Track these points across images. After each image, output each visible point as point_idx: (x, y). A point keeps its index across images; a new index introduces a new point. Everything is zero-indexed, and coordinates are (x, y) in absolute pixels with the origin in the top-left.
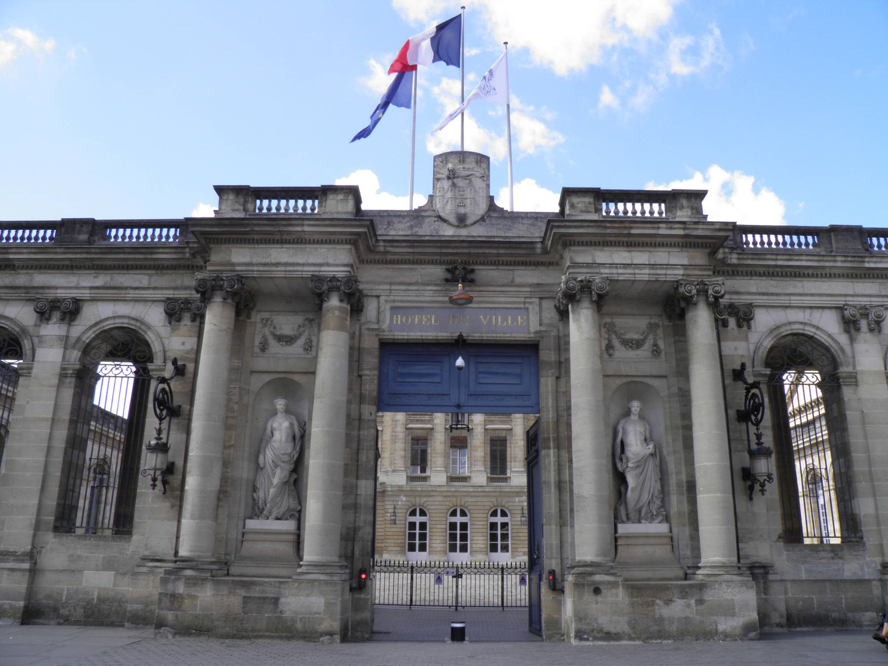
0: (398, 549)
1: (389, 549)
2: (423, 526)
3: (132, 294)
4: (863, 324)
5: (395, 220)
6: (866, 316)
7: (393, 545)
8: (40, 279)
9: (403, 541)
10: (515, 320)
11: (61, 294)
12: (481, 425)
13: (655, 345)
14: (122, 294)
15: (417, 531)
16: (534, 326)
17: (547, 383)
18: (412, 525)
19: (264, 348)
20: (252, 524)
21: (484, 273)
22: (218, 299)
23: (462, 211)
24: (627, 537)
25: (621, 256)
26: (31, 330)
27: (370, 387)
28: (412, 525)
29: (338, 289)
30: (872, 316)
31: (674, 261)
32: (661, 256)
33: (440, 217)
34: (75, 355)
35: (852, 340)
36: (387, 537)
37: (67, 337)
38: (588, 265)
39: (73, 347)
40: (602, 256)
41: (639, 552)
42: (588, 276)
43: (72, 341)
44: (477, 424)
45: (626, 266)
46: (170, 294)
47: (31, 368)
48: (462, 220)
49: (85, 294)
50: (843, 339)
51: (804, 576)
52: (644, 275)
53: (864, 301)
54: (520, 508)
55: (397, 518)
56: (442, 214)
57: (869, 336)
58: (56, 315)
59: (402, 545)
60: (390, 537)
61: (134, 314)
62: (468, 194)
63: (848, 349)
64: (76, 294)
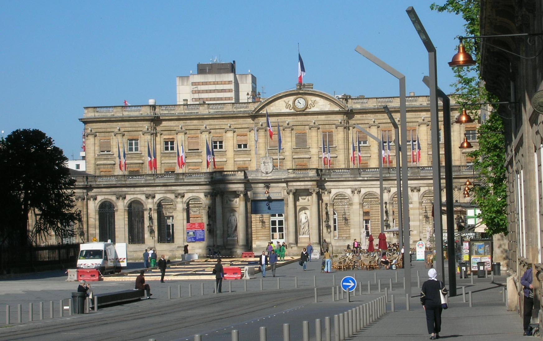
0: (266, 238)
1: (260, 238)
2: (281, 223)
3: (196, 191)
4: (356, 192)
5: (253, 173)
6: (356, 190)
7: (262, 236)
8: (174, 188)
9: (268, 233)
10: (279, 194)
11: (179, 192)
12: (316, 155)
13: (308, 199)
14: (194, 191)
15: (277, 226)
16: (283, 196)
17: (285, 208)
18: (274, 223)
19: (227, 202)
20: (228, 238)
21: (272, 185)
22: (219, 196)
23: (267, 171)
24: (301, 238)
25: (298, 183)
26: (174, 200)
27: (249, 210)
28: (274, 223)
29: (242, 193)
30: (357, 190)
31: (309, 184)
32: (307, 183)
33: (262, 172)
34: (185, 205)
35: (353, 195)
36: (258, 231)
37: (183, 201)
38: (291, 186)
39: (185, 203)
40: (294, 184)
41: (303, 240)
42: (292, 188)
43: (184, 202)
44: (314, 155)
45: (299, 186)
46: (204, 191)
47: (176, 208)
48: (267, 173)
49: (185, 191)
50: (351, 195)
51: (337, 245)
52: (303, 187)
53: (357, 187)
54: (343, 209)
55: (264, 219)
56: (263, 171)
57: (357, 194)
58: (180, 197)
59: (269, 235)
60: (260, 231)
61: (197, 195)
62: (268, 167)
63: (352, 198)
64: (182, 192)
